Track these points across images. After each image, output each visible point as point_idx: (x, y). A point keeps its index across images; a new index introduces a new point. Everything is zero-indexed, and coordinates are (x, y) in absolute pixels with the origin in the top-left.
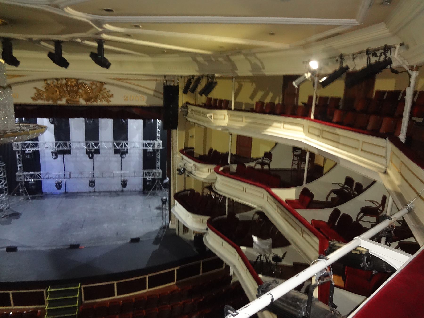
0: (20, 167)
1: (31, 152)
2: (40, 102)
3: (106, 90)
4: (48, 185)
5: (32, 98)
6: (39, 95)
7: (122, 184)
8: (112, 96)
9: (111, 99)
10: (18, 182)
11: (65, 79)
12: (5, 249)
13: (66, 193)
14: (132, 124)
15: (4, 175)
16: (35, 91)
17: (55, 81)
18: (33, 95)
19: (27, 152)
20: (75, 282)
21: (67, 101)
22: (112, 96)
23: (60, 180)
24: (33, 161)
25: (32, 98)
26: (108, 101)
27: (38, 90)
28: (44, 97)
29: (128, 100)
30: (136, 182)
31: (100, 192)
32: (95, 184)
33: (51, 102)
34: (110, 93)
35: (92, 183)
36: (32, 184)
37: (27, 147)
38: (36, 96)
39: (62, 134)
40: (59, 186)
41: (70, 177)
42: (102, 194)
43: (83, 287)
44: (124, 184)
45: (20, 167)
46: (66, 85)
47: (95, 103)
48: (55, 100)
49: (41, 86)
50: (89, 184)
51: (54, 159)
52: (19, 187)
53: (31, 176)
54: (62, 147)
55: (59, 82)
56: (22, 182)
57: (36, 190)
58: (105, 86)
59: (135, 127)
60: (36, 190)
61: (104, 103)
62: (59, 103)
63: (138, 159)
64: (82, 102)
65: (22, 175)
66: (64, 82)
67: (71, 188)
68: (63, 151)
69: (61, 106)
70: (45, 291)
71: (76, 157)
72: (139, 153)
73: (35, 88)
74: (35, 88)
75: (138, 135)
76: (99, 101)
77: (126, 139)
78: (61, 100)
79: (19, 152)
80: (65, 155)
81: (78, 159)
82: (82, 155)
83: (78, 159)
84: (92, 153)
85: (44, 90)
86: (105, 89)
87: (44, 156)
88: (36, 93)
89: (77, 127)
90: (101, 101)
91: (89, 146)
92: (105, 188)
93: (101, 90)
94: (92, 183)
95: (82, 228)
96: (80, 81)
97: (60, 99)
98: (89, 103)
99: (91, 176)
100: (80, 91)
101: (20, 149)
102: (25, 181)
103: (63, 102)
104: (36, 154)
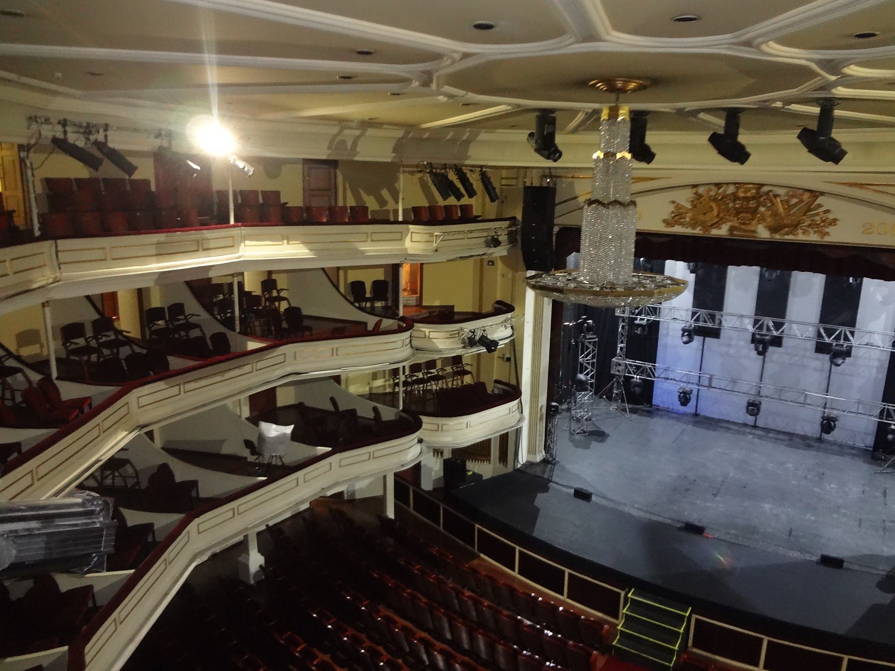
0: (621, 348)
1: (644, 322)
2: (678, 229)
3: (821, 209)
4: (665, 393)
5: (665, 221)
6: (678, 216)
7: (822, 424)
8: (834, 222)
10: (614, 376)
11: (735, 184)
12: (572, 491)
13: (696, 415)
14: (872, 289)
15: (593, 357)
16: (672, 208)
17: (713, 187)
18: (666, 217)
19: (637, 322)
20: (683, 601)
21: (732, 229)
22: (835, 220)
23: (688, 387)
24: (645, 342)
25: (665, 221)
27: (678, 207)
28: (688, 219)
30: (859, 426)
31: (767, 430)
32: (759, 410)
33: (698, 231)
34: (831, 216)
35: (753, 408)
36: (637, 385)
37: (640, 313)
39: (710, 296)
40: (685, 398)
41: (710, 386)
42: (771, 435)
43: (694, 617)
44: (828, 424)
45: (621, 348)
46: (734, 196)
47: (790, 237)
48: (707, 227)
49: (684, 198)
50: (748, 407)
51: (685, 343)
52: (613, 385)
53: (638, 367)
54: (705, 321)
55: (721, 191)
56: (620, 377)
57: (640, 397)
58: (819, 201)
59: (879, 297)
60: (640, 397)
61: (813, 237)
62: (715, 232)
63: (874, 371)
64: (763, 233)
65: (621, 364)
66: (731, 189)
67: (708, 409)
68: (704, 330)
69: (718, 240)
70: (623, 594)
71: (729, 346)
72: (879, 360)
73: (674, 202)
74: (674, 202)
75: (883, 317)
76: (800, 231)
77: (851, 322)
79: (623, 321)
80: (707, 339)
81: (732, 351)
82: (742, 343)
83: (732, 351)
84: (764, 343)
85: (689, 206)
86: (820, 206)
87: (667, 335)
88: (673, 212)
89: (742, 284)
91: (761, 328)
92: (780, 424)
93: (809, 210)
94: (753, 408)
95: (715, 495)
96: (765, 189)
97: (717, 225)
98: (777, 237)
99: (753, 392)
100: (762, 209)
101: (626, 315)
102: (625, 376)
103: (722, 231)
104: (654, 327)
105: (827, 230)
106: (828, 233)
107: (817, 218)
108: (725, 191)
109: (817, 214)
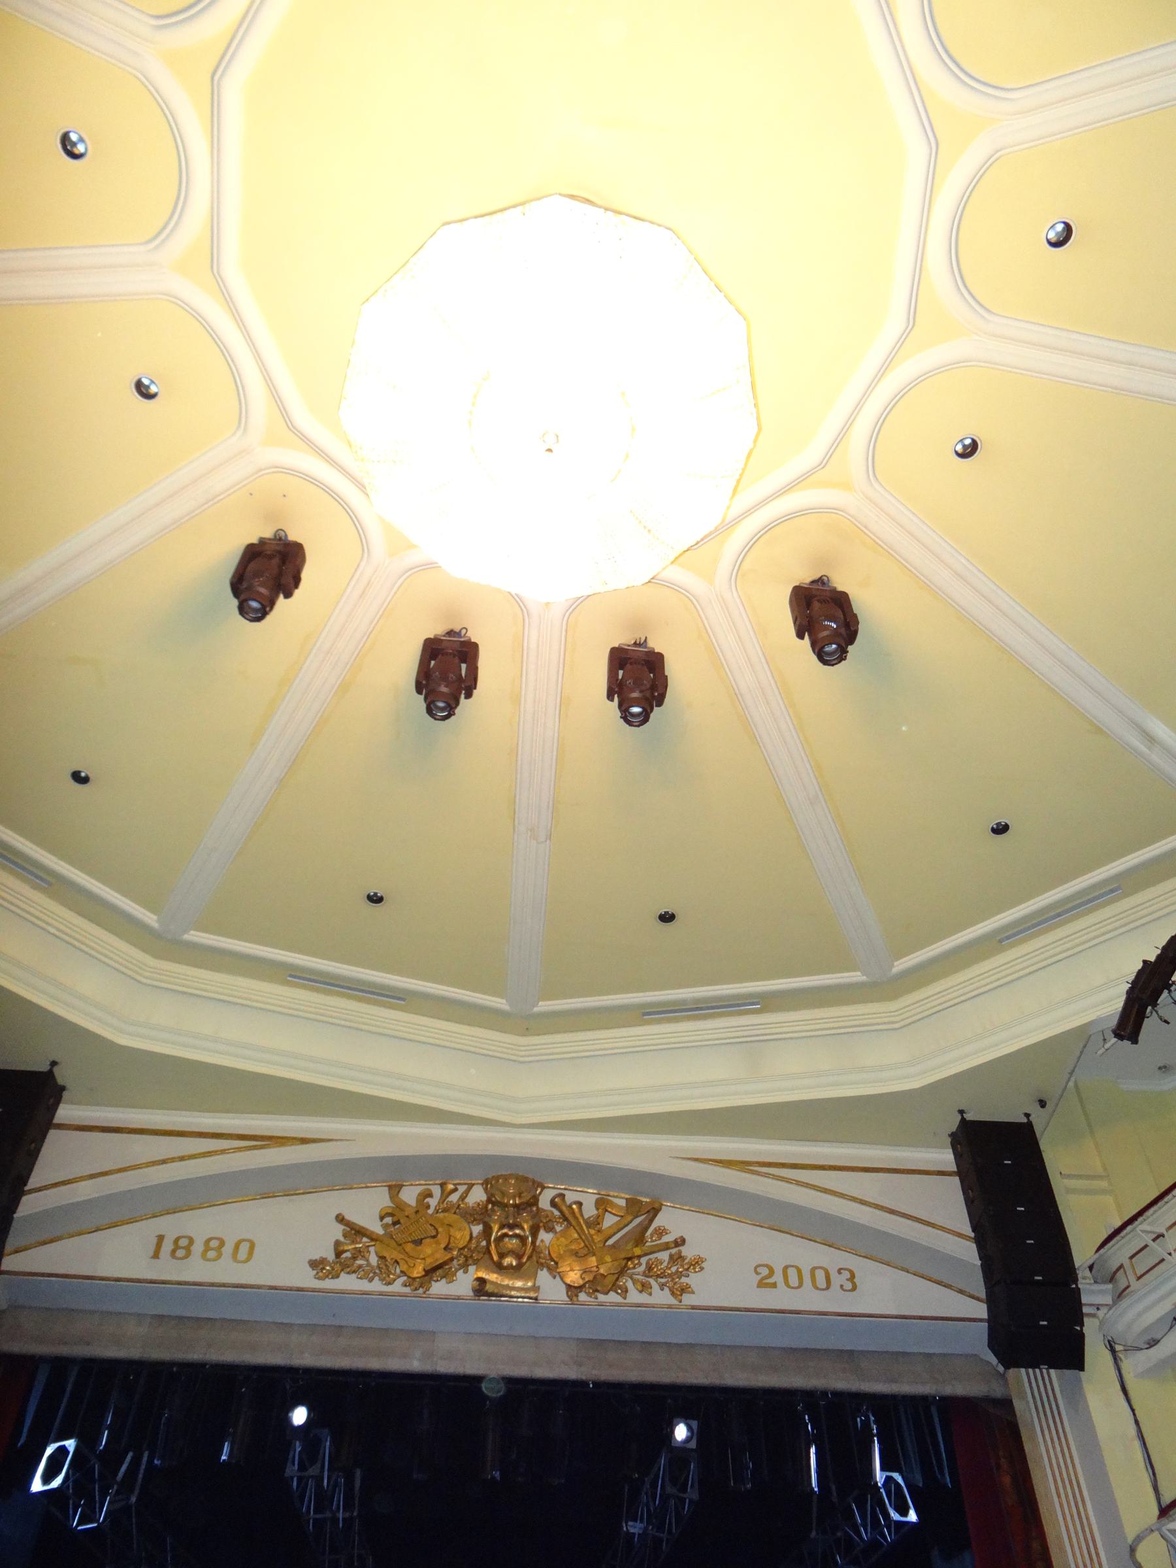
3: (665, 1239)
5: (314, 1264)
9: (693, 1280)
16: (338, 1232)
25: (314, 1264)
26: (681, 1291)
27: (355, 1231)
28: (374, 1260)
29: (774, 1285)
38: (338, 1254)
55: (454, 1198)
61: (661, 1297)
66: (478, 1196)
73: (340, 1219)
74: (340, 1219)
78: (449, 1276)
86: (661, 1232)
88: (337, 1243)
90: (644, 1288)
100: (544, 1237)
105: (684, 1280)
106: (685, 1289)
107: (664, 1256)
108: (463, 1198)
109: (666, 1247)
